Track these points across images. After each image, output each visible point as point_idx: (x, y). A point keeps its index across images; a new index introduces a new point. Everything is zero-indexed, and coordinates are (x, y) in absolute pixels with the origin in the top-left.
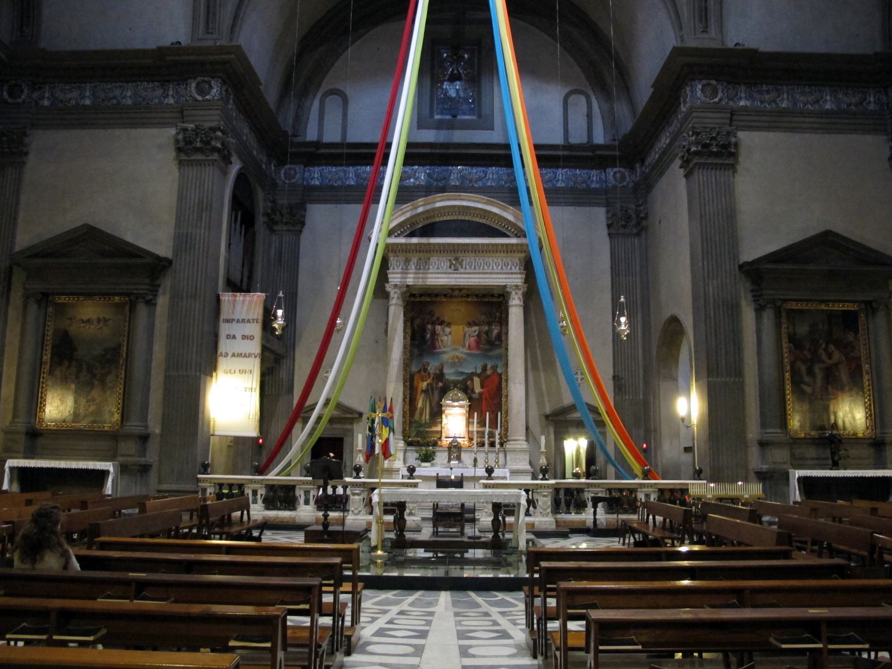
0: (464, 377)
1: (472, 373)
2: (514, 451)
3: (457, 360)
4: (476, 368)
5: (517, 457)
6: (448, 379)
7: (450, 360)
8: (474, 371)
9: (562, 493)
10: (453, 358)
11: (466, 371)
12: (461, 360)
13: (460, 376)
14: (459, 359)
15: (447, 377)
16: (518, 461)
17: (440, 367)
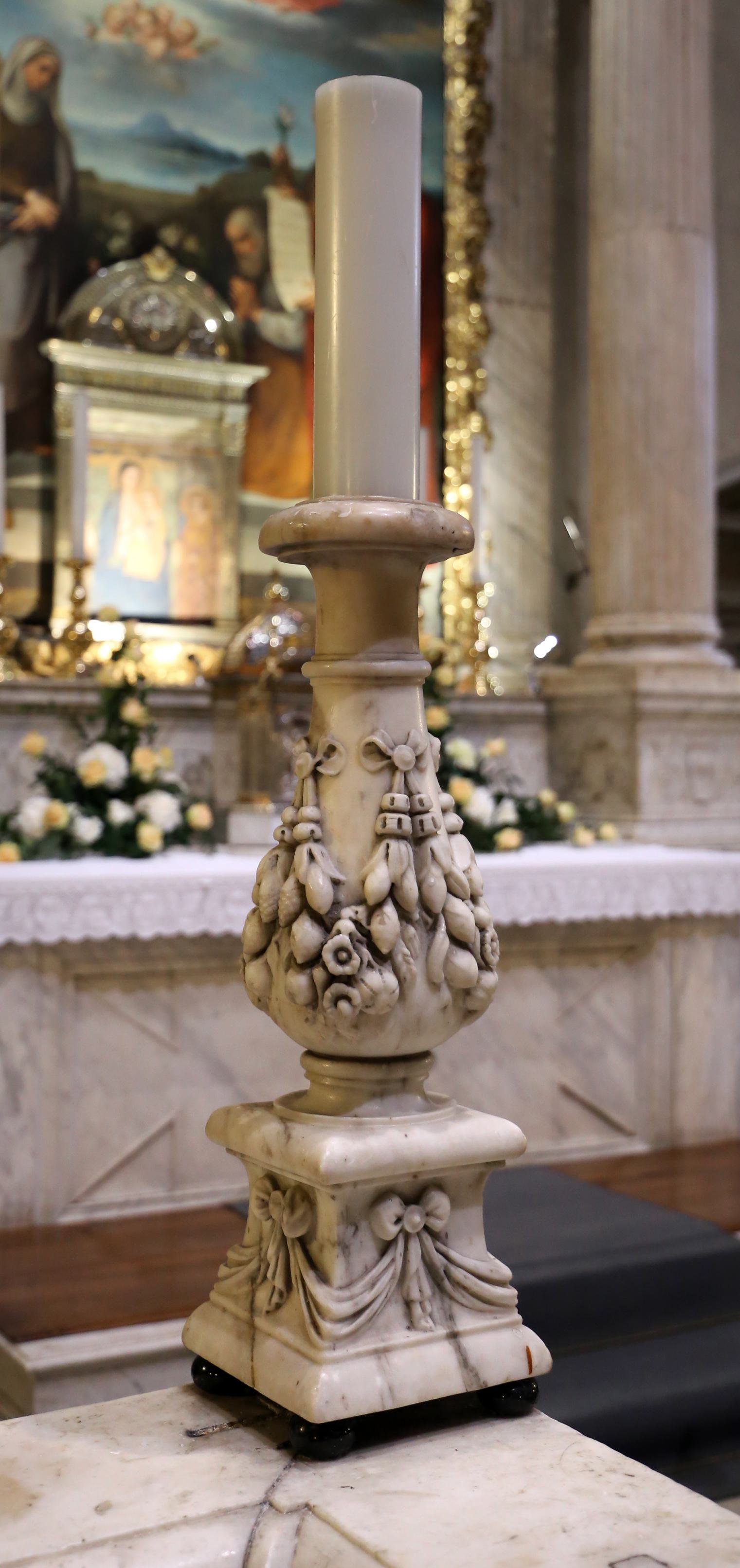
0: (210, 178)
1: (260, 160)
2: (685, 715)
3: (157, 47)
4: (283, 128)
5: (702, 758)
6: (90, 175)
7: (106, 37)
8: (271, 147)
9: (491, 933)
10: (126, 26)
11: (221, 141)
12: (186, 52)
13: (177, 169)
14: (172, 42)
15: (84, 160)
16: (703, 790)
17: (35, 75)
